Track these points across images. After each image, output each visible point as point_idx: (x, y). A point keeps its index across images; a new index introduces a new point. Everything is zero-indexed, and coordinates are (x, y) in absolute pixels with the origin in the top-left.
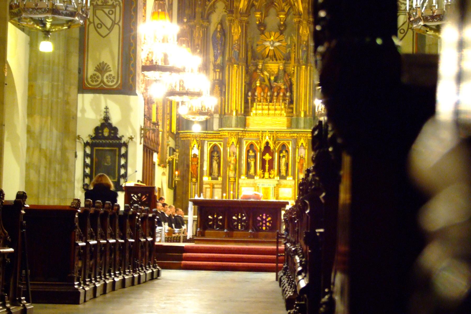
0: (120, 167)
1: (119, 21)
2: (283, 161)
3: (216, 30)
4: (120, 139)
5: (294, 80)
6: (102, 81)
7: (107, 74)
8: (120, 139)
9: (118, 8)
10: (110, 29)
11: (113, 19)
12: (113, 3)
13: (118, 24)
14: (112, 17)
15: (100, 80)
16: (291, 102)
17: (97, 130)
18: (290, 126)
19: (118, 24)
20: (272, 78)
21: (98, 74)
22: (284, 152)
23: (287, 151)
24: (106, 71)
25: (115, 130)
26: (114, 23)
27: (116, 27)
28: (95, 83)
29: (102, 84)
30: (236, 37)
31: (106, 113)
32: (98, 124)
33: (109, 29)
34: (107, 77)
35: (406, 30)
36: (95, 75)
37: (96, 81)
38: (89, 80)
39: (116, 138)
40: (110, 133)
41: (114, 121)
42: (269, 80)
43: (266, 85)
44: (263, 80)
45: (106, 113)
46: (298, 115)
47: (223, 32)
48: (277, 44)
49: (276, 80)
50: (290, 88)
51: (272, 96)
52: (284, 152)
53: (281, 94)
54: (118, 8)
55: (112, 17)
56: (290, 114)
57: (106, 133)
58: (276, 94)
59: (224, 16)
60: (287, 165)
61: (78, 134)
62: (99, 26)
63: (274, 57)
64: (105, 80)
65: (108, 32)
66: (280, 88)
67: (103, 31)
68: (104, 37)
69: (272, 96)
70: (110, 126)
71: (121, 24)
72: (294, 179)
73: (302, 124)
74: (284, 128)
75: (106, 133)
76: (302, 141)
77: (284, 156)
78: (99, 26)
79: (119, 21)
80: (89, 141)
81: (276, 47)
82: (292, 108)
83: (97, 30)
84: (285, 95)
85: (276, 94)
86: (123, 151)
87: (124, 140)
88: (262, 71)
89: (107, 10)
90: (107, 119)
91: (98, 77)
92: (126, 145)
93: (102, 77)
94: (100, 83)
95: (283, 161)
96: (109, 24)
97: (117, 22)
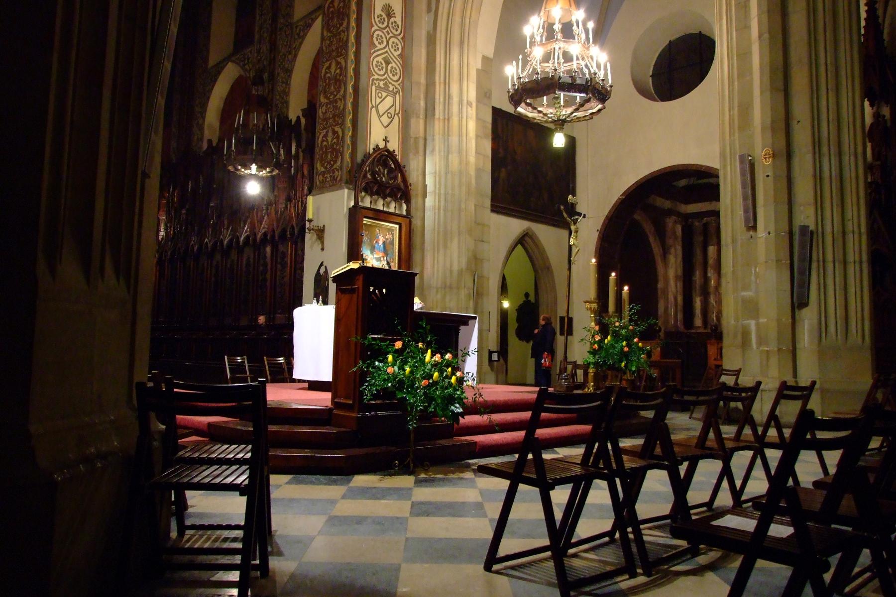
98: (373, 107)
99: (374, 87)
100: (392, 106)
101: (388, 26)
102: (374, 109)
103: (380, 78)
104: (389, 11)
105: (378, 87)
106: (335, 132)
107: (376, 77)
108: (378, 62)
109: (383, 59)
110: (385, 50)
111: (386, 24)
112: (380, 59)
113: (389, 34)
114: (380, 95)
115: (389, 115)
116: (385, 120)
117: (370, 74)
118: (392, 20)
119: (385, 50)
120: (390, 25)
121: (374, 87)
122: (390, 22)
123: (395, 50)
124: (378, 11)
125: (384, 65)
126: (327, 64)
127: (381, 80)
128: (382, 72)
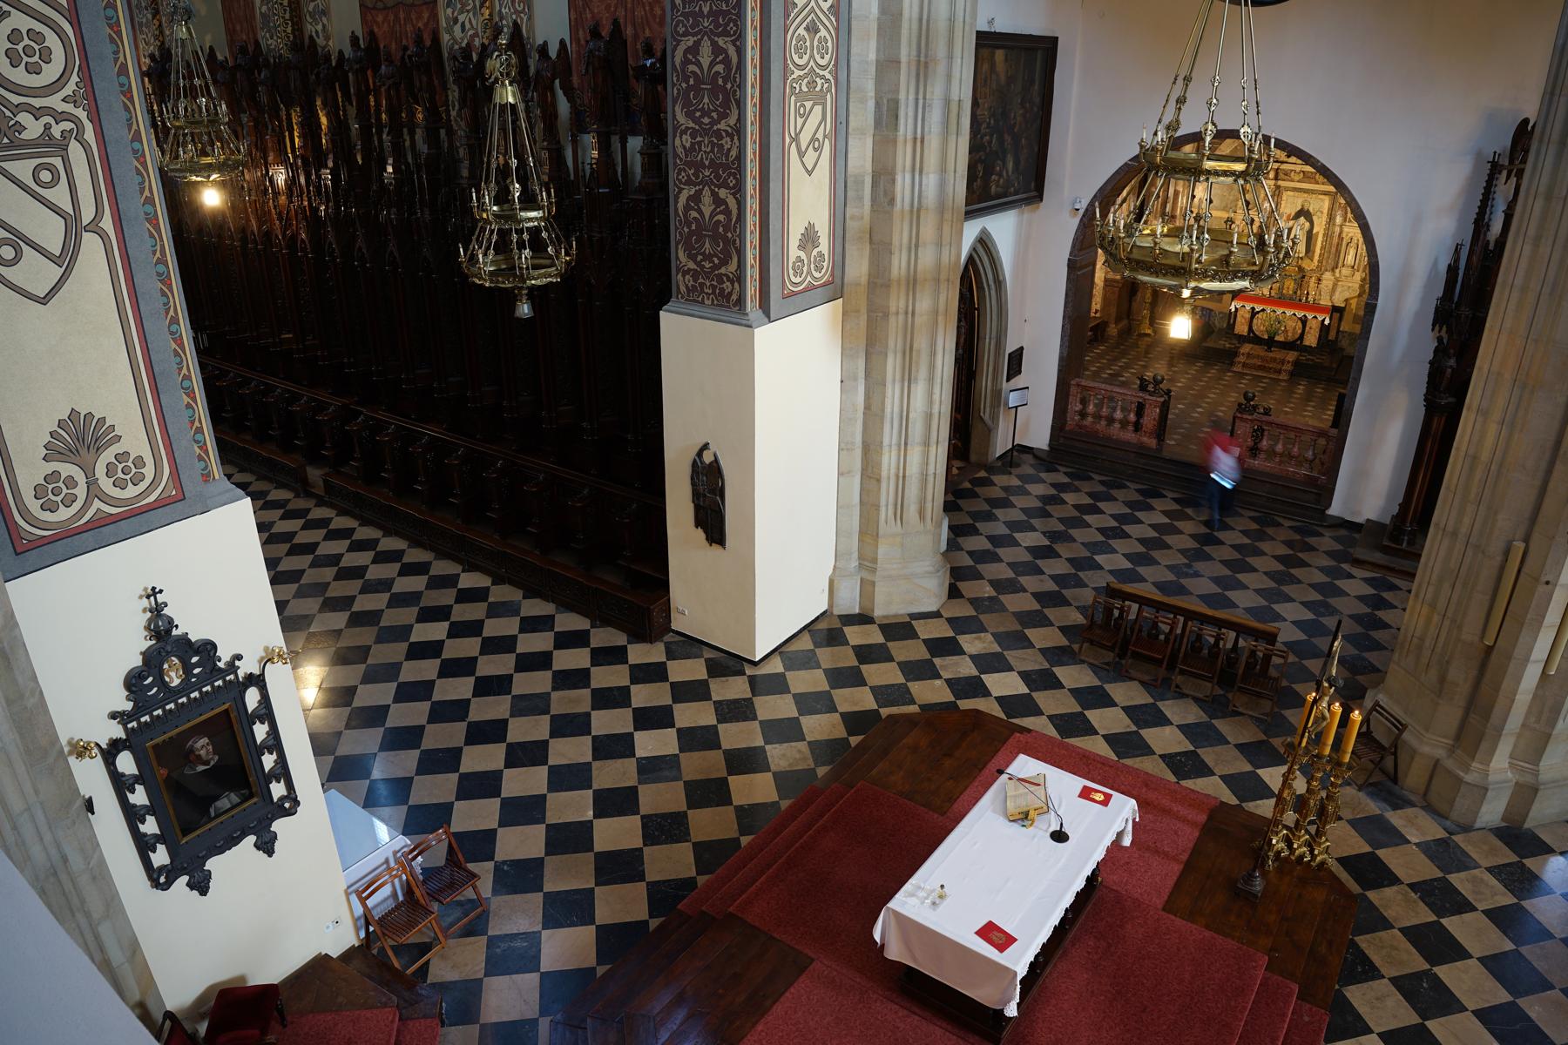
0: (260, 750)
4: (232, 667)
7: (108, 456)
8: (232, 667)
9: (75, 149)
10: (67, 258)
12: (47, 127)
13: (94, 227)
17: (133, 682)
21: (67, 469)
25: (208, 648)
26: (74, 228)
27: (90, 242)
29: (97, 504)
31: (157, 611)
36: (53, 477)
38: (34, 506)
39: (212, 671)
40: (187, 668)
41: (191, 626)
45: (157, 611)
55: (60, 195)
68: (44, 301)
70: (186, 647)
80: (117, 731)
86: (252, 698)
87: (247, 667)
89: (23, 169)
90: (161, 628)
91: (71, 482)
92: (258, 680)
94: (87, 504)
96: (51, 233)
97: (87, 215)
106: (718, 201)
109: (807, 29)
126: (690, 41)
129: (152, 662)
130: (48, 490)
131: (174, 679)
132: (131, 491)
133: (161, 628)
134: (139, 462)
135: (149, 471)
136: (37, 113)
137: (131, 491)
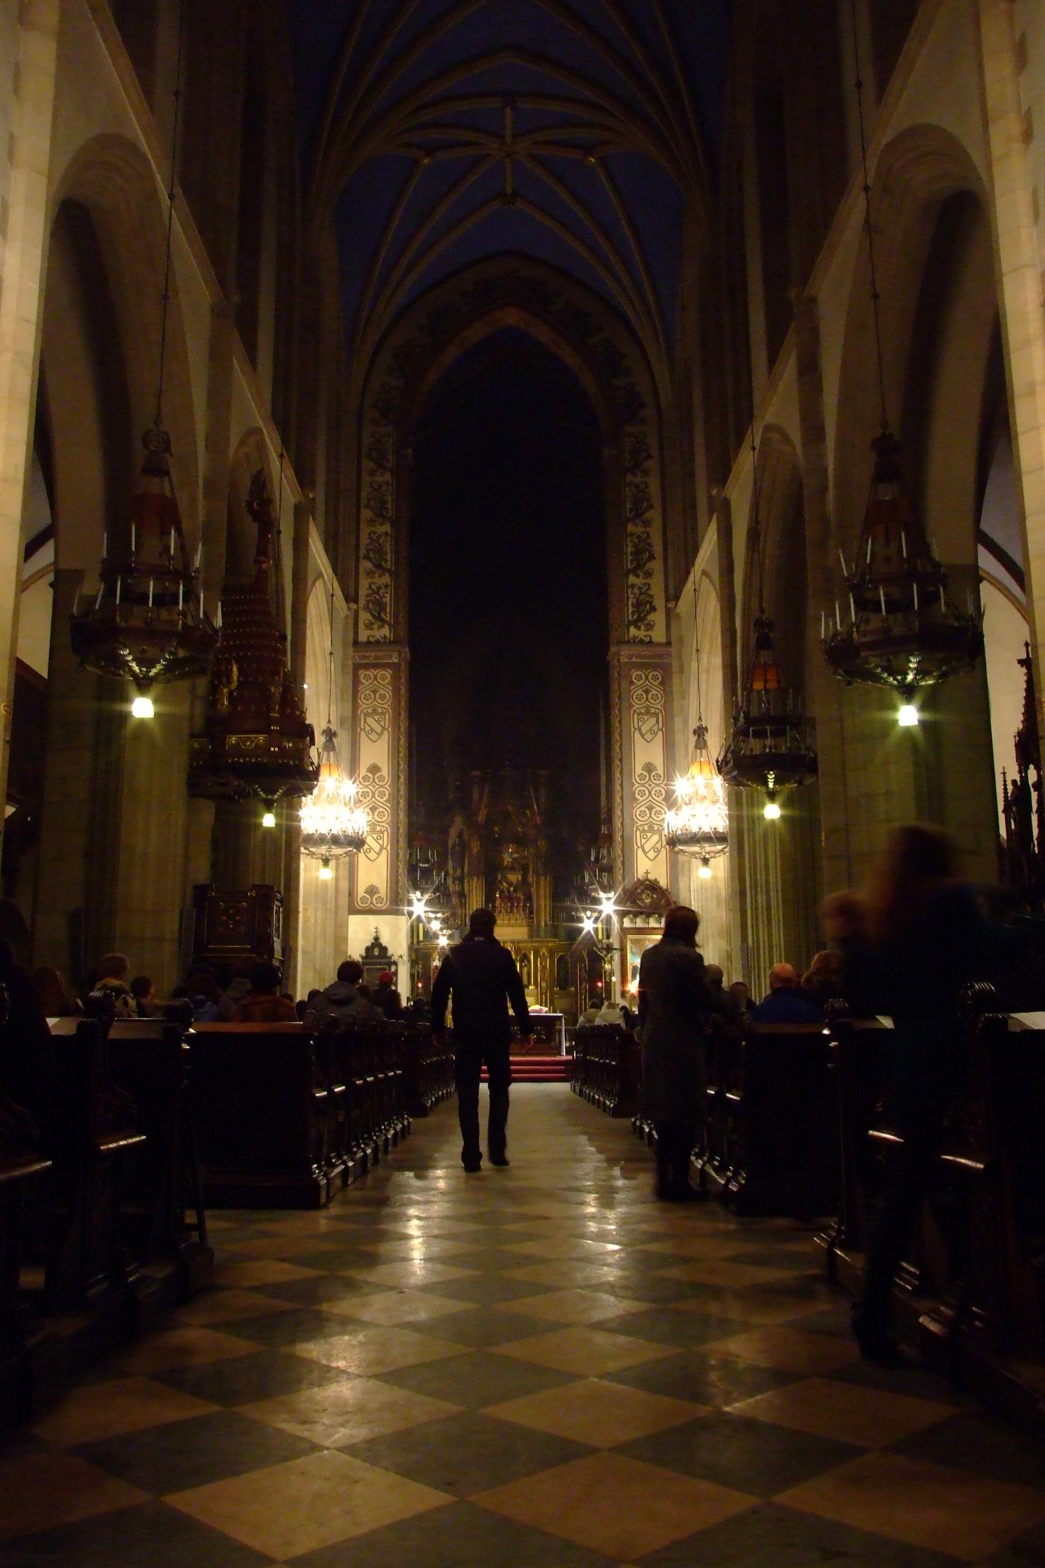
1: (387, 846)
2: (526, 969)
3: (454, 845)
5: (533, 890)
6: (372, 903)
10: (379, 854)
11: (381, 844)
14: (381, 842)
15: (369, 902)
16: (531, 912)
17: (369, 950)
18: (531, 936)
19: (386, 848)
20: (512, 889)
22: (526, 961)
23: (529, 961)
24: (375, 893)
25: (384, 950)
26: (382, 848)
28: (364, 905)
30: (475, 850)
32: (369, 944)
33: (377, 854)
34: (376, 899)
35: (659, 848)
37: (366, 903)
38: (359, 902)
41: (384, 941)
42: (509, 891)
43: (506, 897)
44: (502, 892)
45: (376, 932)
46: (539, 925)
47: (463, 846)
48: (515, 856)
49: (515, 891)
50: (529, 898)
51: (512, 907)
52: (526, 961)
53: (522, 904)
54: (386, 834)
55: (381, 842)
56: (530, 926)
57: (376, 952)
58: (516, 904)
59: (462, 829)
60: (529, 974)
61: (349, 954)
62: (368, 851)
63: (512, 869)
64: (374, 901)
65: (377, 856)
66: (520, 898)
67: (372, 855)
69: (512, 907)
71: (389, 848)
72: (537, 987)
73: (542, 934)
74: (526, 937)
75: (376, 952)
76: (544, 950)
77: (526, 965)
78: (368, 851)
79: (387, 846)
81: (514, 859)
82: (533, 918)
83: (366, 856)
84: (525, 906)
85: (516, 904)
88: (501, 882)
90: (377, 939)
91: (368, 899)
93: (372, 899)
95: (526, 969)
96: (377, 848)
97: (385, 846)
98: (638, 847)
99: (638, 833)
100: (658, 842)
101: (650, 779)
102: (640, 851)
103: (644, 823)
104: (649, 768)
105: (644, 831)
107: (640, 823)
108: (641, 811)
110: (648, 800)
111: (647, 779)
112: (643, 808)
113: (650, 785)
114: (645, 837)
115: (656, 850)
116: (652, 854)
117: (633, 822)
118: (654, 773)
119: (648, 800)
120: (652, 778)
121: (638, 833)
122: (652, 775)
123: (659, 797)
124: (639, 769)
125: (648, 812)
127: (645, 825)
128: (646, 818)
129: (373, 946)
130: (363, 899)
131: (376, 953)
132: (379, 905)
133: (377, 939)
134: (383, 899)
135: (384, 902)
136: (380, 826)
137: (379, 905)
